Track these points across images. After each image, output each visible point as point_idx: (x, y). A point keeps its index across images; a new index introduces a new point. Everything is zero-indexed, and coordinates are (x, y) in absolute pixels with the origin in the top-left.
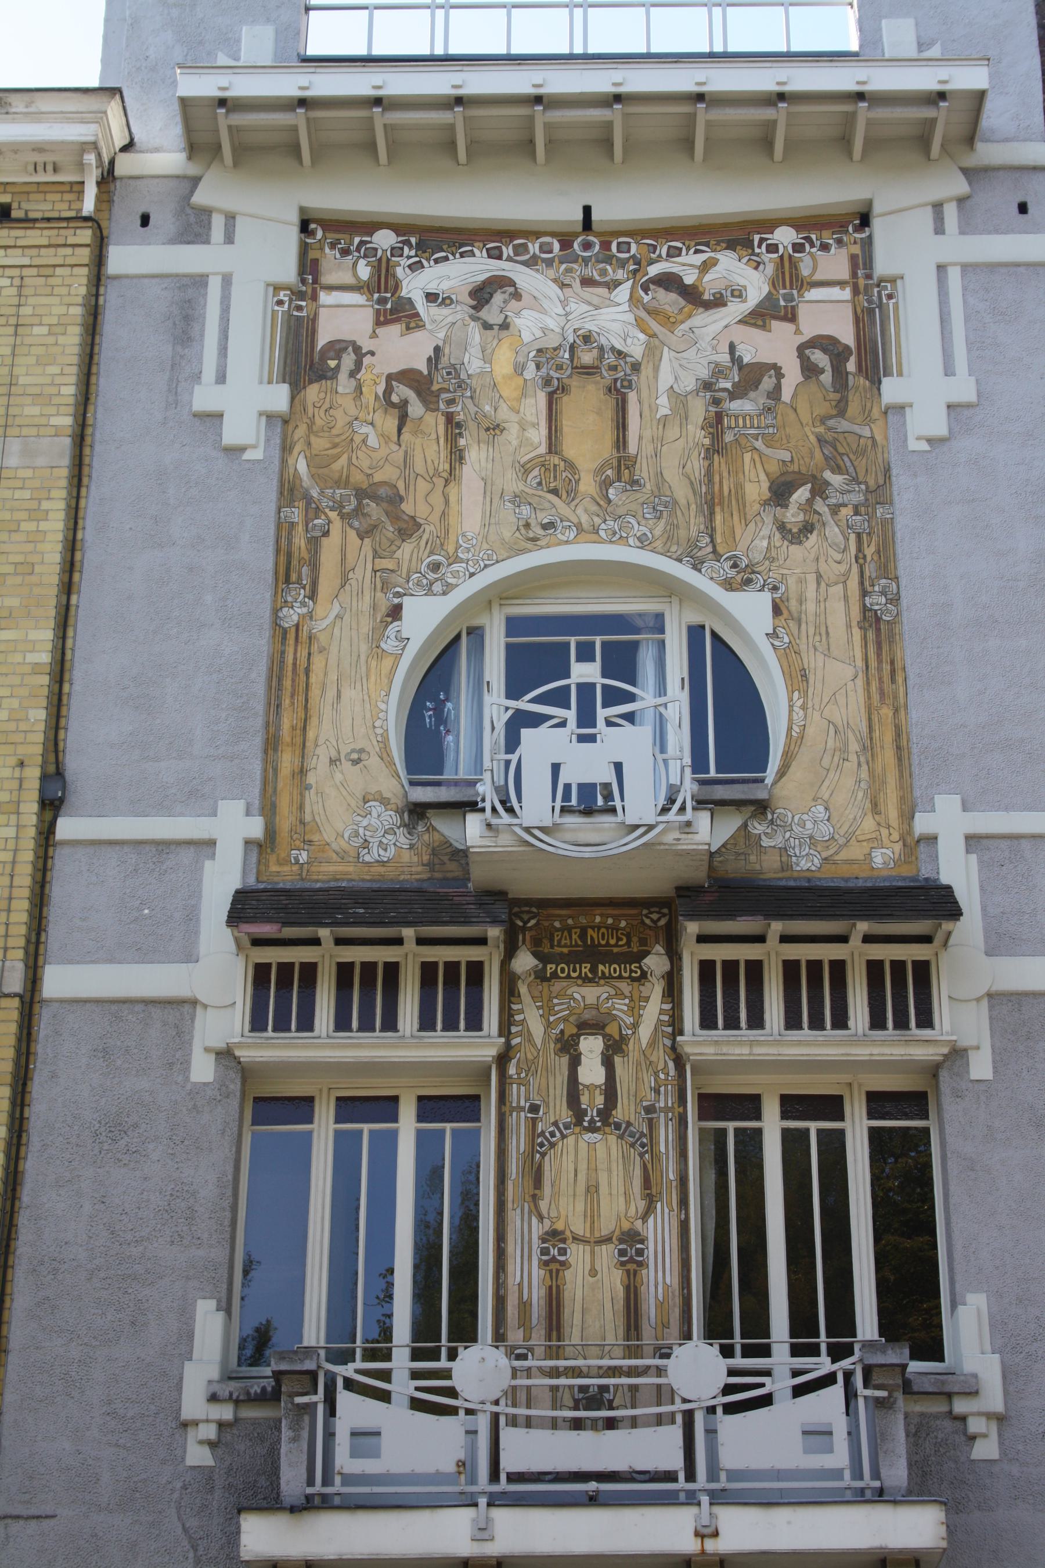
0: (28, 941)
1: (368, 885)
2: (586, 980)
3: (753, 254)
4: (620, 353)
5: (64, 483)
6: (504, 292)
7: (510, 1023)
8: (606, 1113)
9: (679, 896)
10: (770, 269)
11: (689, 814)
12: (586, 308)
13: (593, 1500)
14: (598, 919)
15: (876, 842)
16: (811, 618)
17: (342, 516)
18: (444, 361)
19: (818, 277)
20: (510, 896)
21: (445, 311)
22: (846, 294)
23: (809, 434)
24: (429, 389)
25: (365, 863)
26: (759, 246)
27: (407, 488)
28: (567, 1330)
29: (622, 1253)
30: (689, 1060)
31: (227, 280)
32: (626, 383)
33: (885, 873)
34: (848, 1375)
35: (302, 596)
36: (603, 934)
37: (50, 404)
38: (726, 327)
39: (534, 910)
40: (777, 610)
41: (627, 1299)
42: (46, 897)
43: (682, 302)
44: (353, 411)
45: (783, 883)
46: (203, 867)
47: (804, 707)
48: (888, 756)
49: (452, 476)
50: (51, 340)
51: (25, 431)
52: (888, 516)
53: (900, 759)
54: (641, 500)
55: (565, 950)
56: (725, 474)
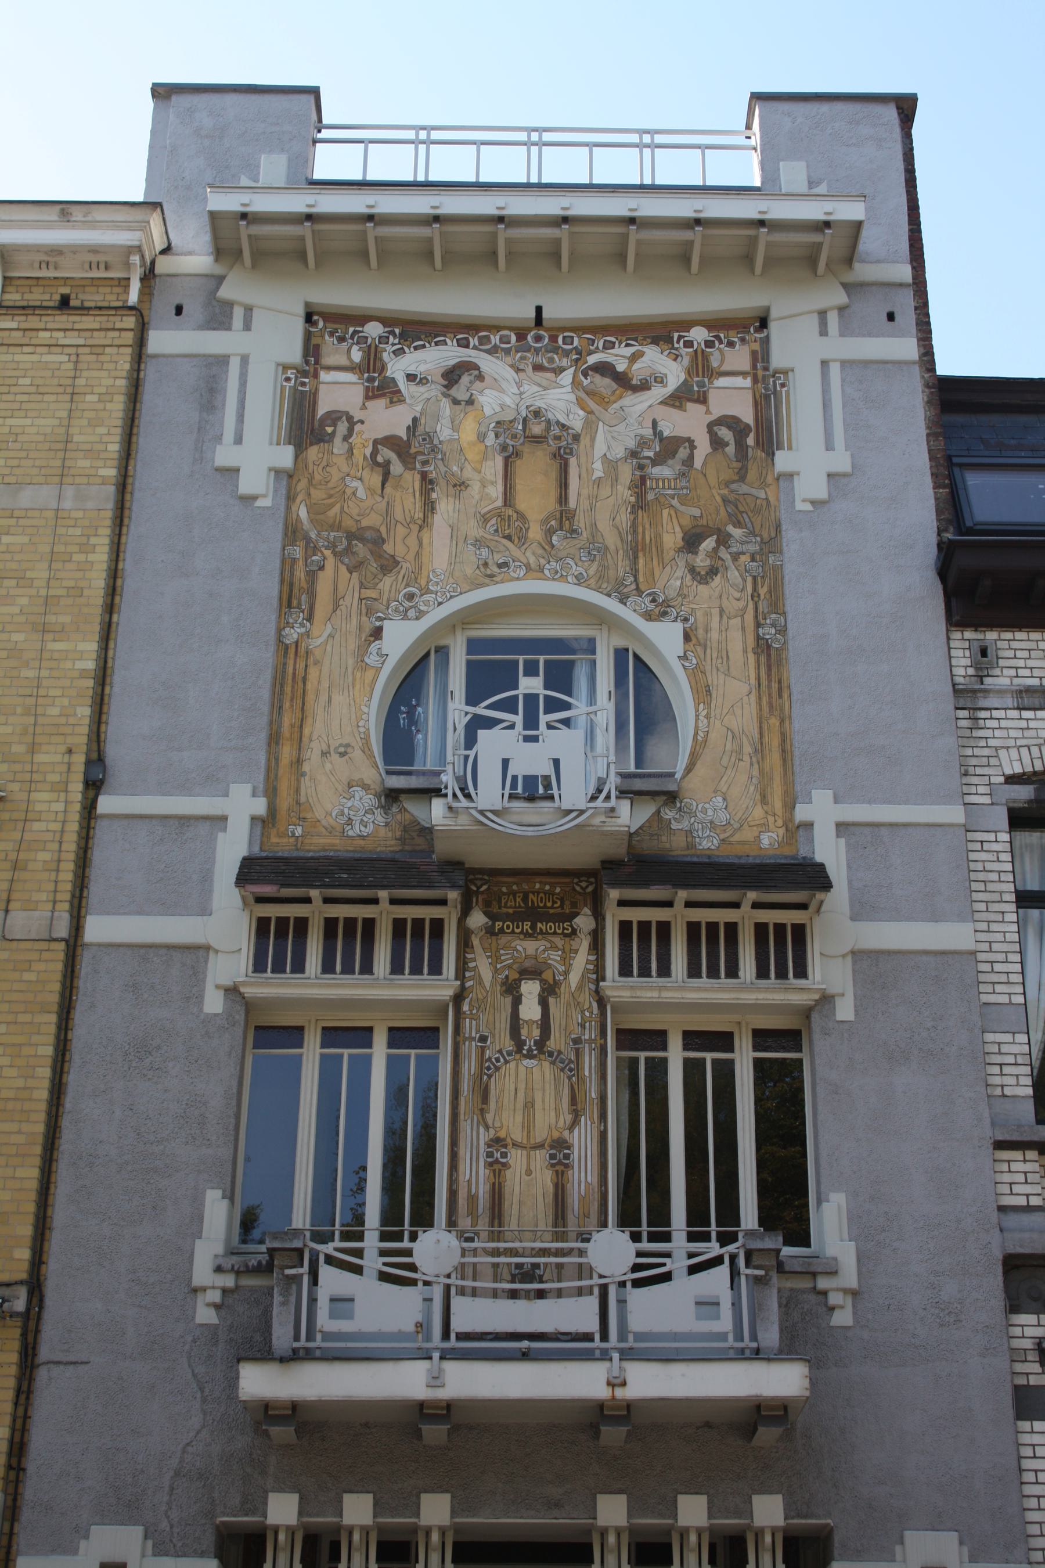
0: (73, 896)
2: (527, 935)
3: (673, 348)
4: (563, 426)
6: (470, 375)
7: (465, 970)
8: (541, 1044)
9: (604, 868)
10: (686, 361)
11: (613, 801)
12: (536, 388)
13: (525, 1356)
14: (538, 886)
15: (765, 827)
16: (715, 645)
17: (335, 554)
18: (420, 429)
19: (724, 368)
20: (467, 866)
21: (422, 389)
22: (748, 382)
23: (716, 495)
24: (408, 452)
25: (348, 836)
26: (678, 342)
27: (388, 531)
28: (506, 1218)
29: (552, 1157)
31: (245, 360)
32: (568, 451)
33: (771, 852)
34: (733, 1258)
35: (301, 619)
37: (98, 458)
38: (650, 407)
39: (486, 877)
40: (687, 637)
41: (556, 1195)
42: (88, 860)
43: (615, 386)
44: (345, 469)
45: (688, 859)
47: (708, 717)
48: (774, 758)
49: (425, 523)
50: (100, 406)
51: (78, 480)
52: (778, 563)
53: (784, 760)
54: (579, 546)
55: (511, 911)
56: (647, 526)
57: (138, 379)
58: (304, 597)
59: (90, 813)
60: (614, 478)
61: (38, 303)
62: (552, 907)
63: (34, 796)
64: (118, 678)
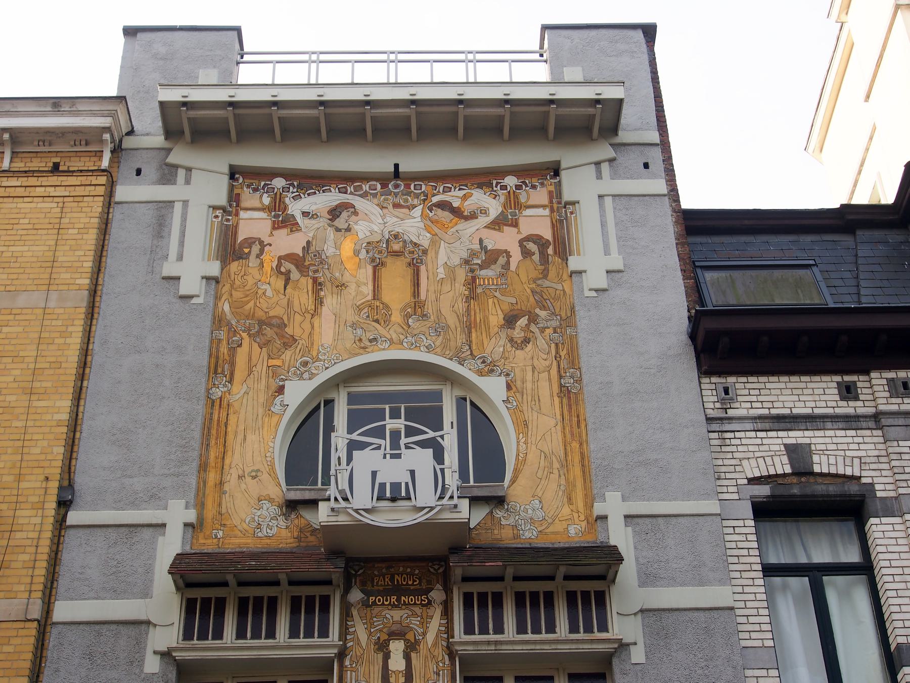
0: (45, 587)
1: (260, 550)
2: (394, 606)
3: (493, 190)
4: (415, 244)
5: (83, 316)
6: (348, 211)
7: (346, 634)
11: (456, 501)
12: (396, 219)
15: (570, 521)
16: (529, 392)
17: (250, 335)
18: (312, 249)
19: (529, 203)
21: (313, 222)
22: (547, 212)
23: (527, 288)
26: (496, 187)
27: (289, 319)
30: (457, 653)
31: (185, 203)
32: (419, 261)
33: (577, 539)
35: (224, 381)
36: (404, 578)
40: (509, 387)
42: (58, 560)
43: (452, 217)
44: (258, 277)
45: (515, 546)
46: (157, 541)
47: (526, 443)
48: (577, 470)
49: (316, 313)
50: (80, 236)
51: (61, 287)
52: (574, 334)
53: (584, 472)
54: (428, 326)
55: (381, 588)
56: (478, 311)
57: (107, 219)
58: (226, 366)
59: (61, 525)
60: (452, 278)
61: (37, 169)
62: (413, 585)
63: (18, 513)
64: (87, 426)
